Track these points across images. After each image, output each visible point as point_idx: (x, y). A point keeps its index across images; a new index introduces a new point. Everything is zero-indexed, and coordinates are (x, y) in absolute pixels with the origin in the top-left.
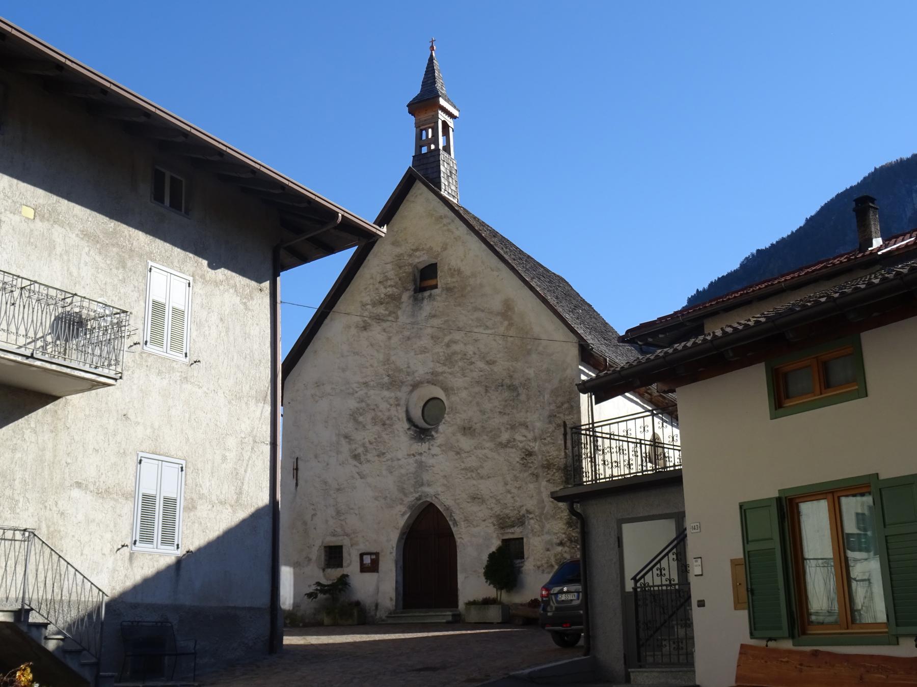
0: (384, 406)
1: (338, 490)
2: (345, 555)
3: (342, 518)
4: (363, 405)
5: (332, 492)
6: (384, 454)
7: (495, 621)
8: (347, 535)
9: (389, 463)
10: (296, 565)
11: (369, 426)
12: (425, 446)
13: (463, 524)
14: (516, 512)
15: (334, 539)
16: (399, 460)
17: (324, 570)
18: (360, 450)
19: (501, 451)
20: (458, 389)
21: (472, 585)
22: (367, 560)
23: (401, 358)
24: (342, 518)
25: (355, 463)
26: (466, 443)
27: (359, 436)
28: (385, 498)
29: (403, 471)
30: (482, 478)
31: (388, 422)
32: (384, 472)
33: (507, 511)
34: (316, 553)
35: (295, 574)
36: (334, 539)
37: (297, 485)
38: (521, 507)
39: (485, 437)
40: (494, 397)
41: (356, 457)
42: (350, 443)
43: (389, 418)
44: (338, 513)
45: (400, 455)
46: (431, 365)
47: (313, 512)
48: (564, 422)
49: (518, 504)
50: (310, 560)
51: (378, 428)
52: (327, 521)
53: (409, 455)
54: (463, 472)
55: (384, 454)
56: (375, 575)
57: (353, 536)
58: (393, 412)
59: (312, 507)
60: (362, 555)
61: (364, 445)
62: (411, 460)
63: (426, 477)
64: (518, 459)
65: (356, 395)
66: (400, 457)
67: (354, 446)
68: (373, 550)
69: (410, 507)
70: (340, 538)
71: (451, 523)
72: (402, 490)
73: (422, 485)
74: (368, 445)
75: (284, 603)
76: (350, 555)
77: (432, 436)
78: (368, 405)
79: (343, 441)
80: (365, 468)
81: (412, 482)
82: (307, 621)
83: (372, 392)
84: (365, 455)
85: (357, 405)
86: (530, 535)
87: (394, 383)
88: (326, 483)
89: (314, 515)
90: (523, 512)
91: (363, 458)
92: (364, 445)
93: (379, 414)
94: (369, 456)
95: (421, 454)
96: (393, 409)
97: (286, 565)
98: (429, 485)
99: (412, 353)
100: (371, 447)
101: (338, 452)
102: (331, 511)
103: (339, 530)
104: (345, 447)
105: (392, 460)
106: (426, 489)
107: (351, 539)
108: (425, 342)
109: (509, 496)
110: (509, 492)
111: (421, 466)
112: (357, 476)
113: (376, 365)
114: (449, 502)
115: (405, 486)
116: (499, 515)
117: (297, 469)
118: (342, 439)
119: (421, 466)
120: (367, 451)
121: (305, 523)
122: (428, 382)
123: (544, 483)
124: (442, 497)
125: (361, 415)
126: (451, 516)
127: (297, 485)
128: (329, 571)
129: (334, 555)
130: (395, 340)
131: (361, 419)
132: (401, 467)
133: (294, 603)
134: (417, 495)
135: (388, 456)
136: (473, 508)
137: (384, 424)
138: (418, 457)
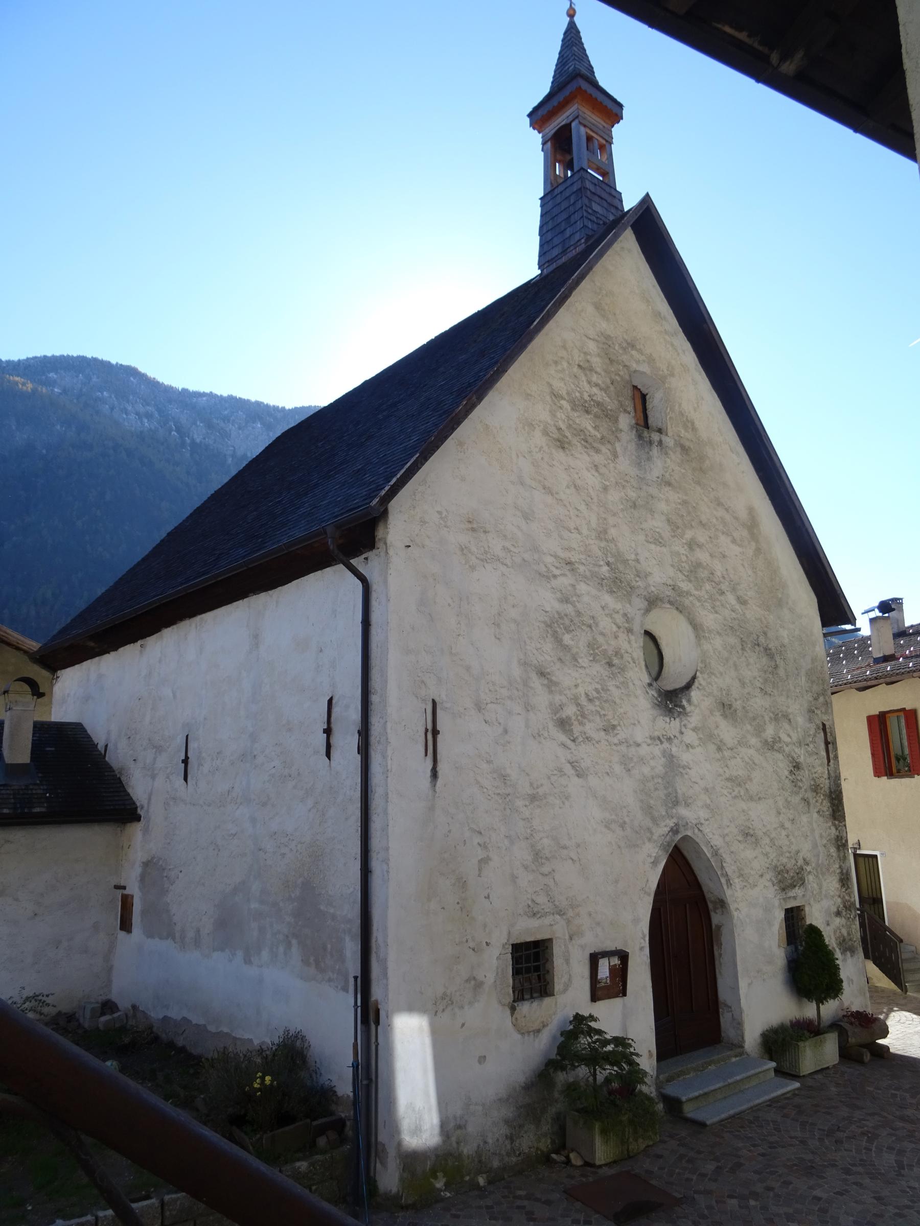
0: (605, 624)
1: (533, 798)
2: (558, 962)
3: (546, 869)
4: (569, 609)
5: (519, 803)
6: (614, 727)
7: (831, 1064)
8: (561, 913)
9: (623, 748)
10: (438, 1007)
11: (584, 661)
12: (676, 724)
13: (737, 881)
14: (793, 861)
15: (534, 923)
16: (639, 745)
17: (513, 1009)
18: (570, 711)
19: (769, 754)
20: (710, 631)
21: (759, 997)
22: (604, 971)
23: (627, 541)
24: (546, 869)
25: (563, 738)
26: (727, 732)
27: (566, 676)
28: (623, 826)
29: (646, 770)
30: (751, 798)
31: (616, 661)
32: (618, 769)
33: (785, 860)
34: (495, 966)
35: (436, 1033)
36: (534, 923)
37: (434, 774)
38: (798, 852)
39: (749, 727)
40: (751, 661)
41: (563, 724)
42: (551, 692)
43: (617, 653)
44: (538, 856)
45: (640, 735)
46: (671, 572)
47: (481, 854)
48: (824, 725)
49: (794, 848)
50: (479, 985)
51: (598, 669)
52: (514, 878)
53: (652, 738)
54: (729, 784)
55: (614, 727)
56: (617, 1002)
57: (570, 913)
58: (623, 642)
59: (477, 840)
60: (594, 959)
61: (576, 700)
62: (657, 750)
63: (682, 788)
64: (787, 773)
65: (554, 583)
66: (639, 740)
67: (558, 699)
68: (611, 946)
69: (663, 847)
70: (547, 921)
71: (723, 880)
72: (648, 810)
73: (676, 803)
74: (583, 701)
75: (417, 1131)
76: (567, 961)
77: (683, 707)
78: (579, 614)
79: (536, 683)
80: (585, 753)
81: (661, 794)
82: (496, 1164)
83: (582, 587)
84: (581, 723)
85: (557, 606)
86: (812, 902)
87: (617, 584)
88: (504, 778)
89: (485, 861)
90: (801, 862)
91: (577, 729)
92: (576, 700)
93: (600, 639)
94: (590, 728)
95: (669, 739)
96: (623, 636)
97: (411, 1008)
98: (687, 805)
99: (642, 538)
100: (591, 707)
101: (528, 707)
102: (522, 853)
103: (542, 899)
104: (541, 698)
105: (625, 742)
106: (683, 811)
107: (568, 922)
108: (658, 524)
109: (784, 833)
110: (782, 826)
111: (671, 761)
112: (568, 769)
113: (585, 531)
114: (717, 841)
115: (652, 802)
116: (776, 867)
117: (435, 733)
118: (534, 676)
119: (671, 761)
120: (583, 716)
121: (462, 884)
122: (670, 603)
123: (815, 815)
124: (706, 830)
125: (568, 630)
126: (722, 867)
127: (434, 774)
128: (525, 1008)
129: (531, 966)
130: (614, 496)
131: (567, 639)
132: (642, 760)
133: (443, 1125)
134: (671, 823)
135: (622, 734)
136: (748, 853)
137: (610, 664)
138: (666, 745)
